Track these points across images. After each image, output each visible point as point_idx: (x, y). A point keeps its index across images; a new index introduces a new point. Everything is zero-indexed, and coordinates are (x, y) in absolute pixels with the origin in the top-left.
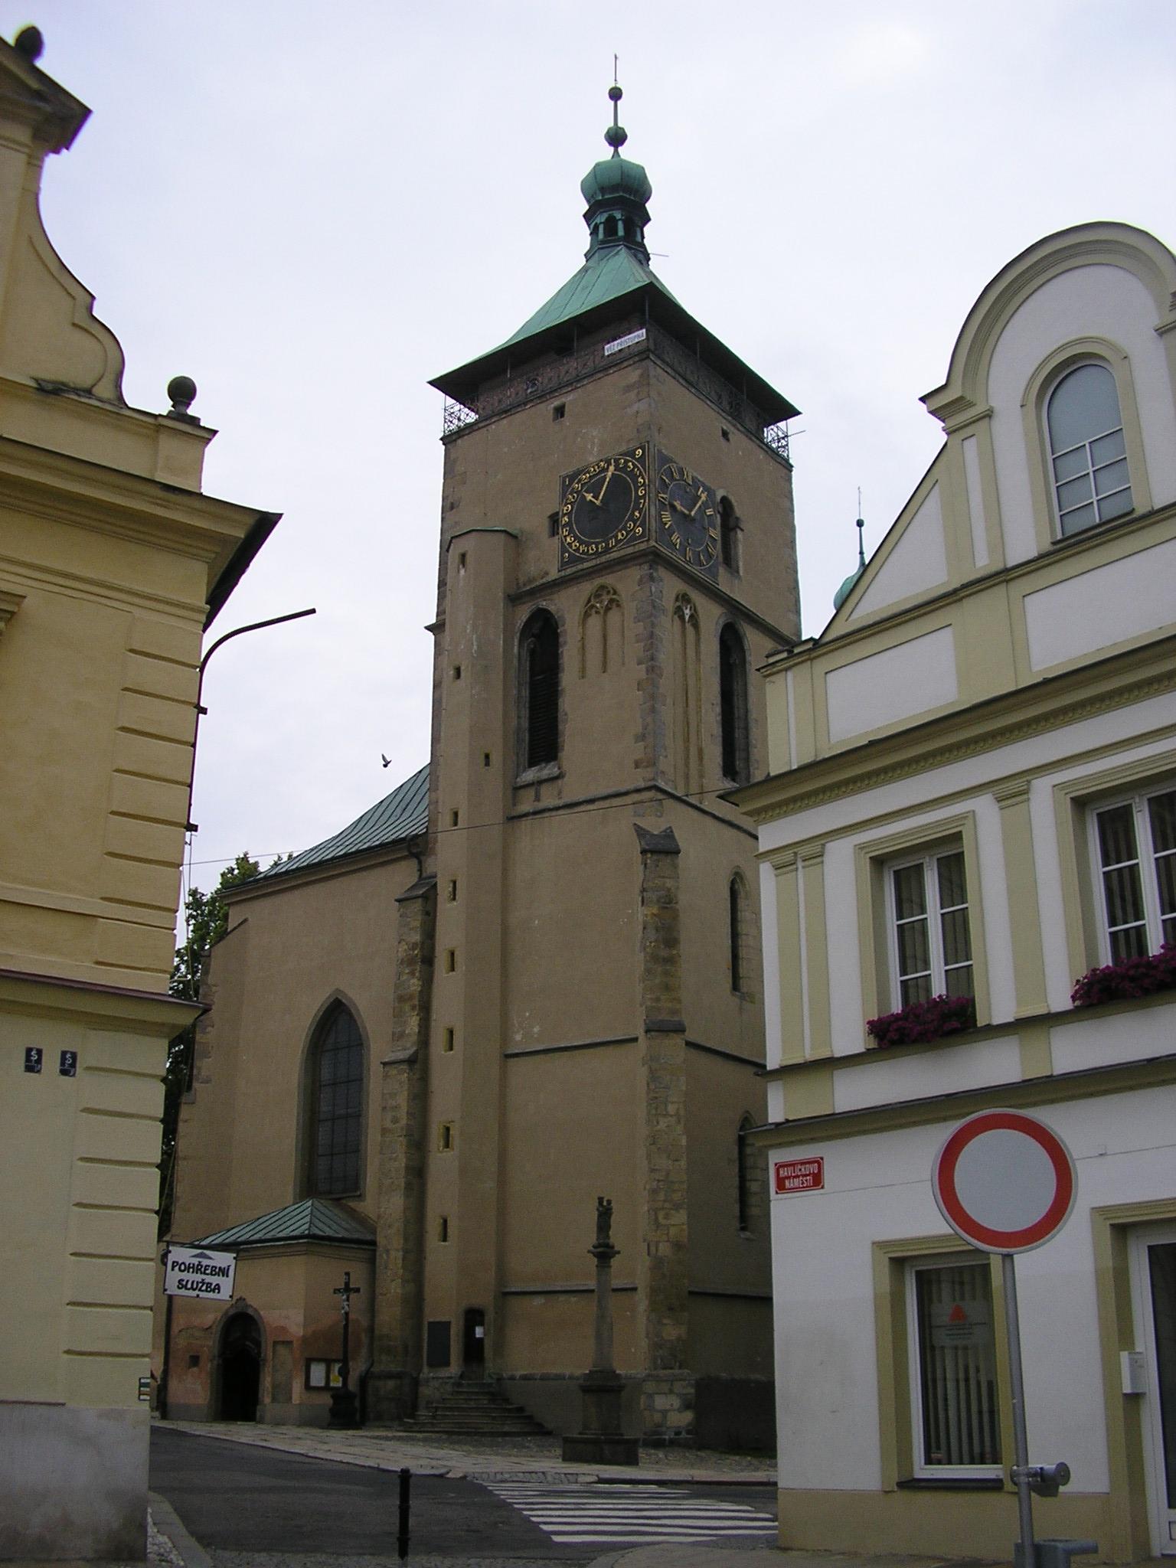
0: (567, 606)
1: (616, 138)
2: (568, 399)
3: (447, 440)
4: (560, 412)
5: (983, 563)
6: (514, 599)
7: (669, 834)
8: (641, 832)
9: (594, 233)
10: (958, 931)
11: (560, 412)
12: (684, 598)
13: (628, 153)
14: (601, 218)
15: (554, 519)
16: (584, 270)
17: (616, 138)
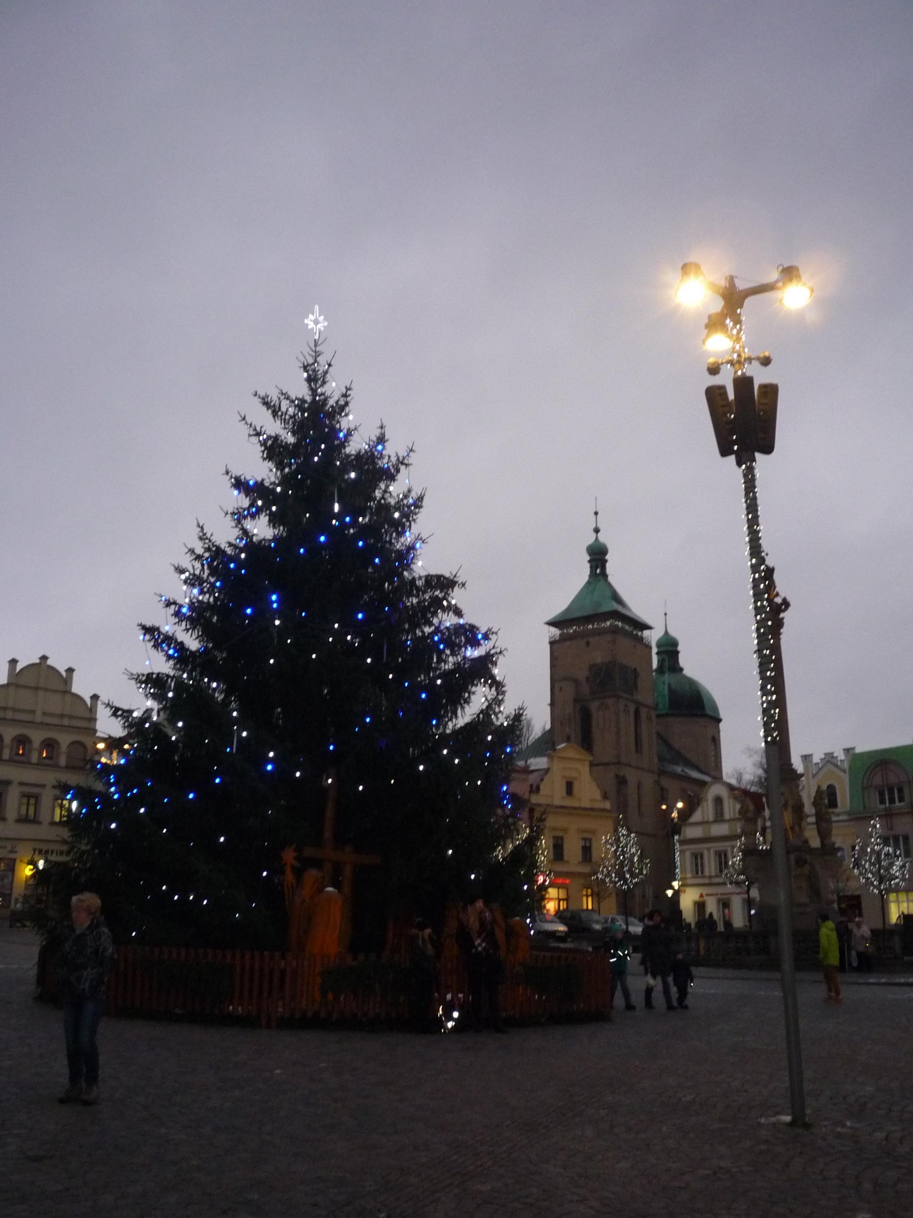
0: (594, 706)
1: (597, 531)
2: (591, 640)
3: (552, 643)
4: (588, 643)
5: (706, 819)
6: (576, 701)
7: (624, 777)
8: (617, 776)
9: (591, 567)
10: (702, 864)
11: (588, 643)
12: (626, 706)
13: (602, 538)
14: (594, 564)
15: (587, 679)
16: (588, 583)
17: (597, 531)
